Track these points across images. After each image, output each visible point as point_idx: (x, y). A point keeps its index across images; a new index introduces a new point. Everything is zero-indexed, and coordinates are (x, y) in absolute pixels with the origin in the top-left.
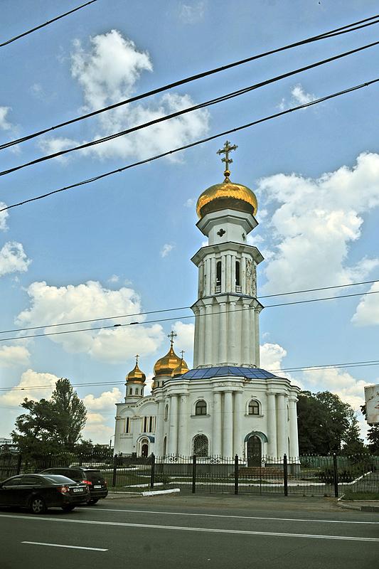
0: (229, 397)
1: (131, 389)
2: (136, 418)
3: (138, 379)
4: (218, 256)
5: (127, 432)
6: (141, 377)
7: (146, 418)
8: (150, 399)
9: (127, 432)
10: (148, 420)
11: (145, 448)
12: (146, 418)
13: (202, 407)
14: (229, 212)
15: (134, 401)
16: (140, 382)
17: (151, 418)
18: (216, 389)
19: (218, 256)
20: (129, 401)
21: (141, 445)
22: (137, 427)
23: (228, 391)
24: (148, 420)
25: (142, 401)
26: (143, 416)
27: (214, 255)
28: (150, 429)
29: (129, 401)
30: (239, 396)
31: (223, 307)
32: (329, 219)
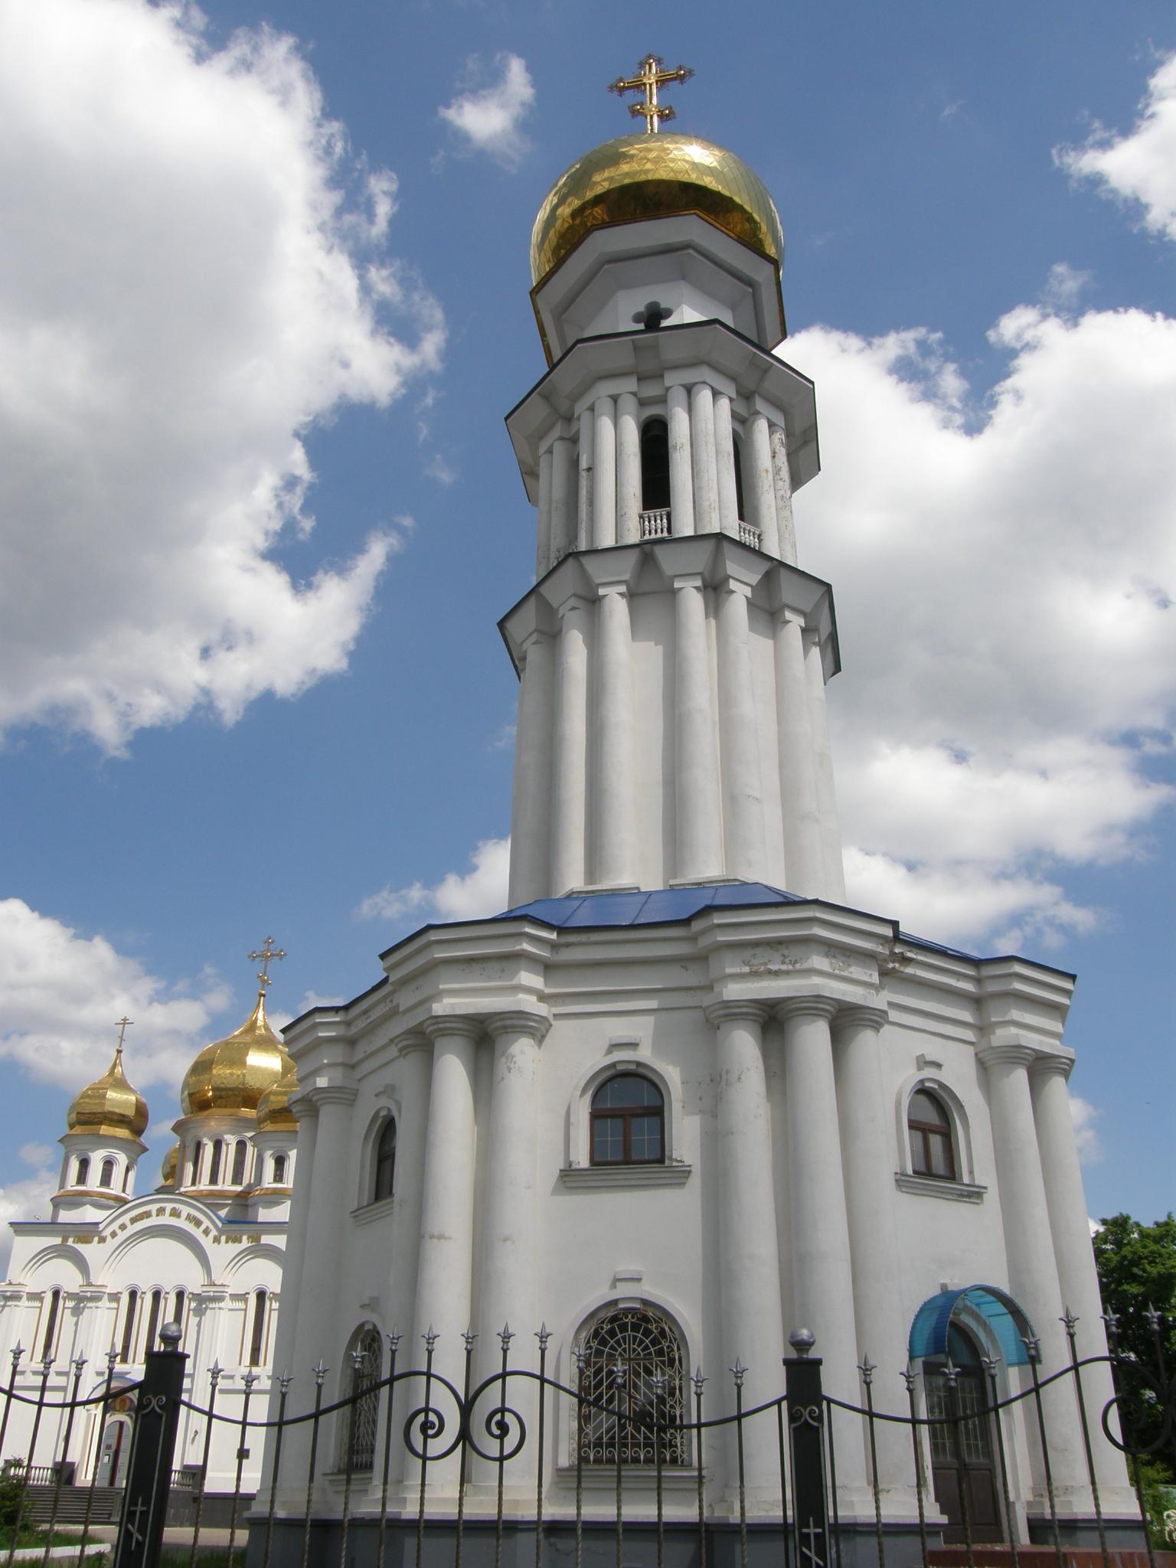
0: (813, 1038)
3: (120, 1120)
4: (651, 390)
8: (161, 1211)
13: (624, 1115)
14: (689, 228)
15: (89, 1214)
16: (123, 1133)
17: (157, 1295)
18: (735, 991)
19: (651, 390)
23: (813, 1006)
25: (125, 1219)
27: (631, 384)
29: (66, 1216)
30: (866, 1043)
31: (693, 601)
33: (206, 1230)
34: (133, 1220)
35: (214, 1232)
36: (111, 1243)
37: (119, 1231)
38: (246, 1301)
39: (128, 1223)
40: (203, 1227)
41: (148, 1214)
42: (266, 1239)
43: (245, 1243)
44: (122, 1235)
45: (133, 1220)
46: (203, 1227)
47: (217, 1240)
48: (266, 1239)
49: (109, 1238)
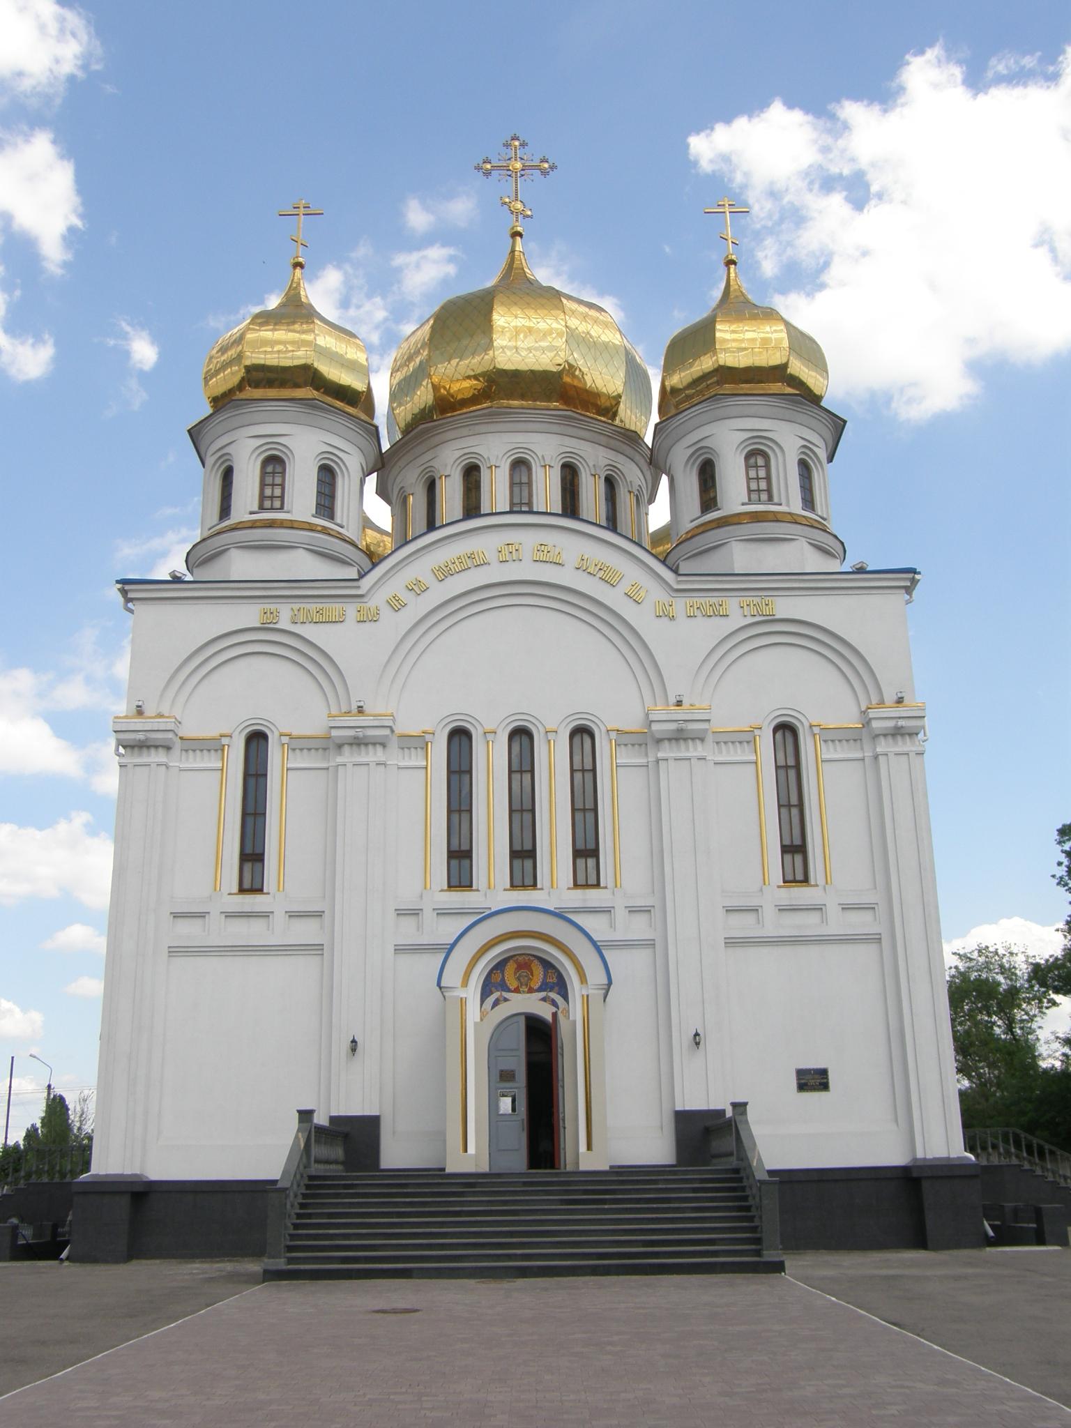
1: (274, 464)
2: (355, 739)
5: (251, 884)
6: (360, 386)
7: (460, 737)
8: (510, 555)
9: (251, 884)
10: (491, 762)
11: (539, 1069)
12: (460, 737)
20: (242, 565)
21: (478, 1020)
22: (370, 833)
24: (491, 762)
26: (423, 710)
28: (523, 855)
32: (550, 298)
33: (634, 585)
34: (444, 573)
35: (654, 594)
36: (392, 625)
37: (405, 596)
38: (752, 742)
39: (428, 579)
40: (624, 586)
41: (474, 562)
42: (786, 607)
43: (737, 620)
44: (418, 607)
45: (444, 573)
46: (624, 586)
47: (666, 614)
48: (786, 607)
49: (386, 612)
